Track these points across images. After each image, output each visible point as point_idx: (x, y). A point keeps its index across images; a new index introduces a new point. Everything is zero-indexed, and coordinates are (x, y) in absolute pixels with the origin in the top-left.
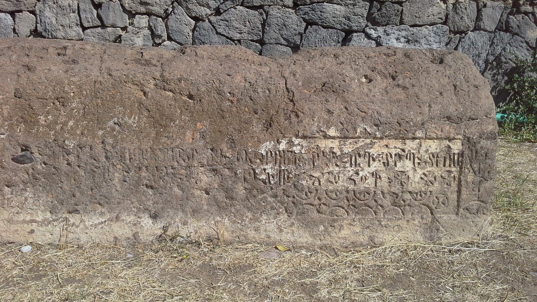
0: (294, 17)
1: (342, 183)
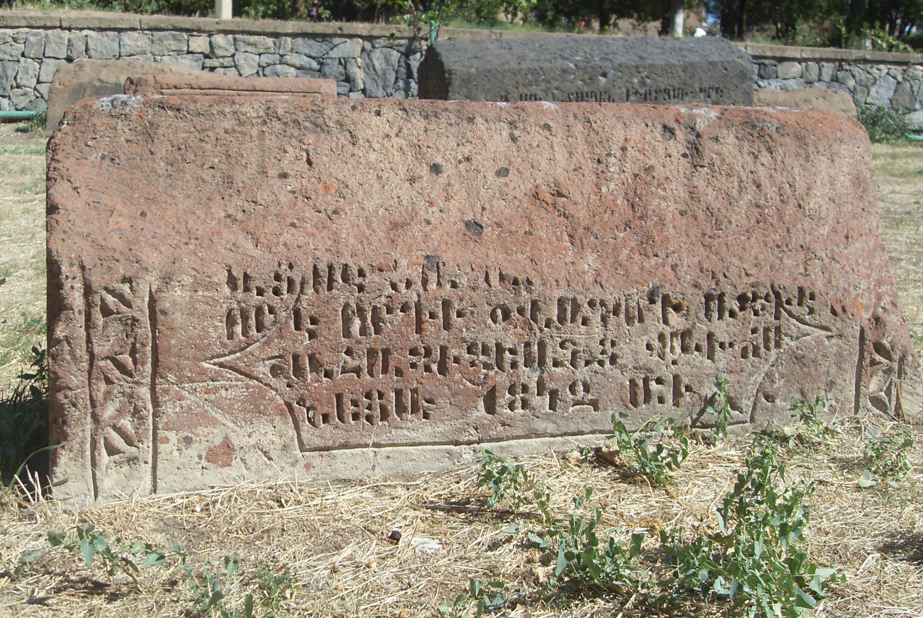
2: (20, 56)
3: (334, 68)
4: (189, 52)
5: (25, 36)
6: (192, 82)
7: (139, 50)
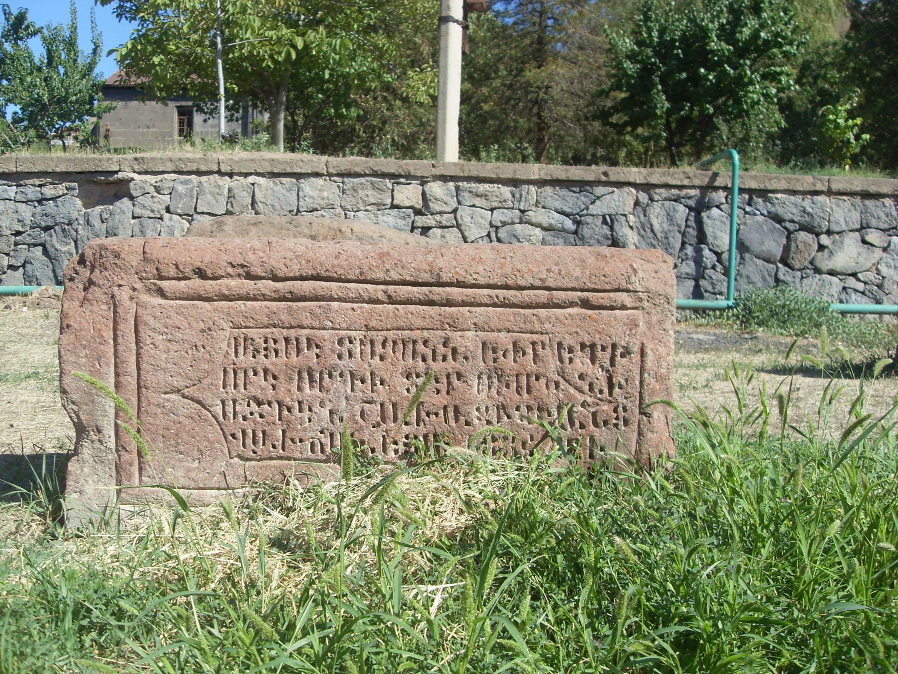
2: (164, 212)
3: (595, 228)
4: (393, 206)
5: (171, 184)
6: (251, 257)
7: (323, 203)
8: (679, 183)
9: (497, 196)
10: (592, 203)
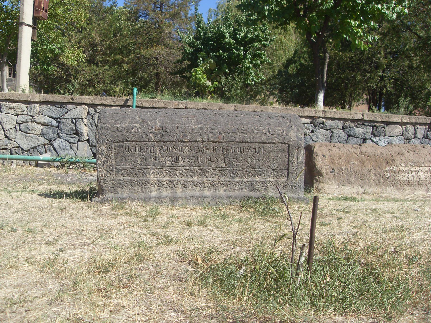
0: (343, 133)
1: (406, 178)
3: (67, 126)
8: (109, 104)
9: (19, 109)
10: (66, 113)
